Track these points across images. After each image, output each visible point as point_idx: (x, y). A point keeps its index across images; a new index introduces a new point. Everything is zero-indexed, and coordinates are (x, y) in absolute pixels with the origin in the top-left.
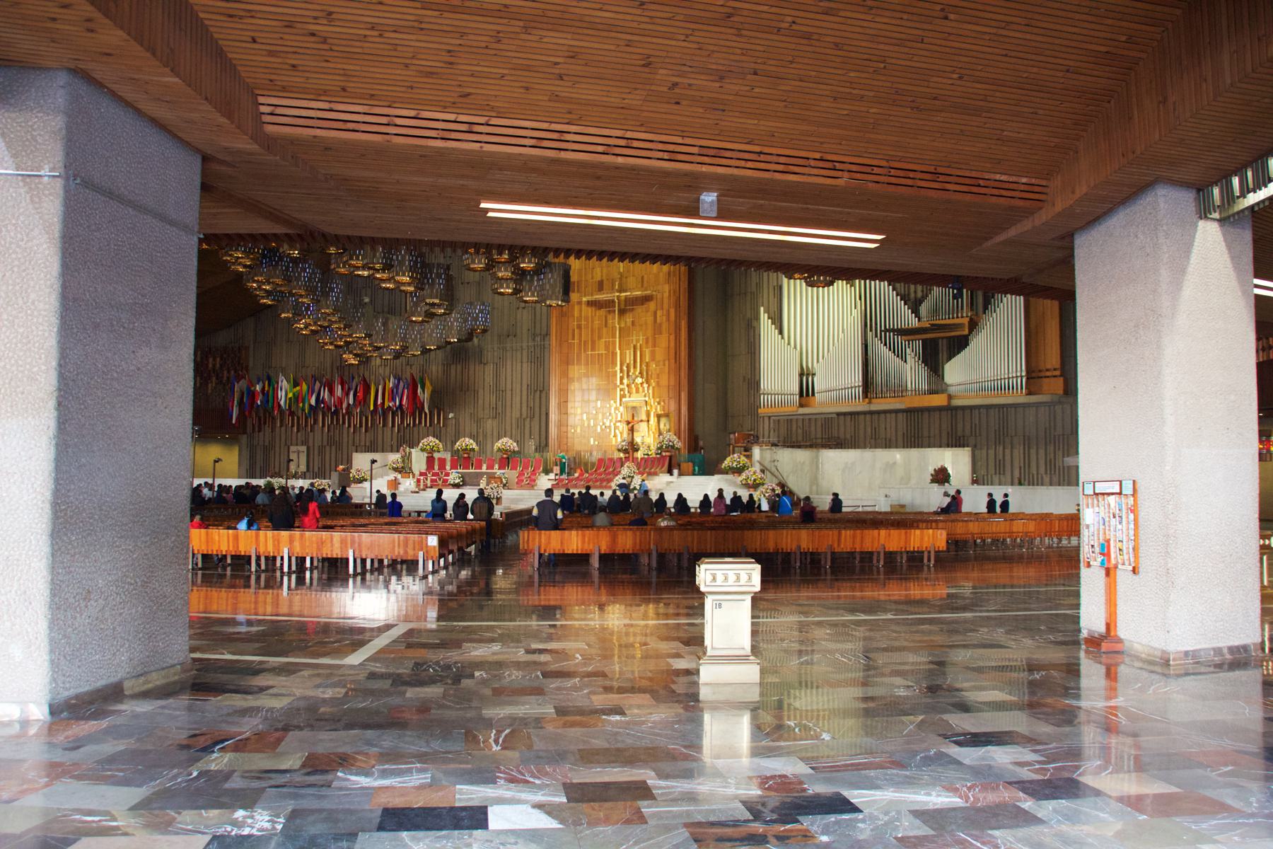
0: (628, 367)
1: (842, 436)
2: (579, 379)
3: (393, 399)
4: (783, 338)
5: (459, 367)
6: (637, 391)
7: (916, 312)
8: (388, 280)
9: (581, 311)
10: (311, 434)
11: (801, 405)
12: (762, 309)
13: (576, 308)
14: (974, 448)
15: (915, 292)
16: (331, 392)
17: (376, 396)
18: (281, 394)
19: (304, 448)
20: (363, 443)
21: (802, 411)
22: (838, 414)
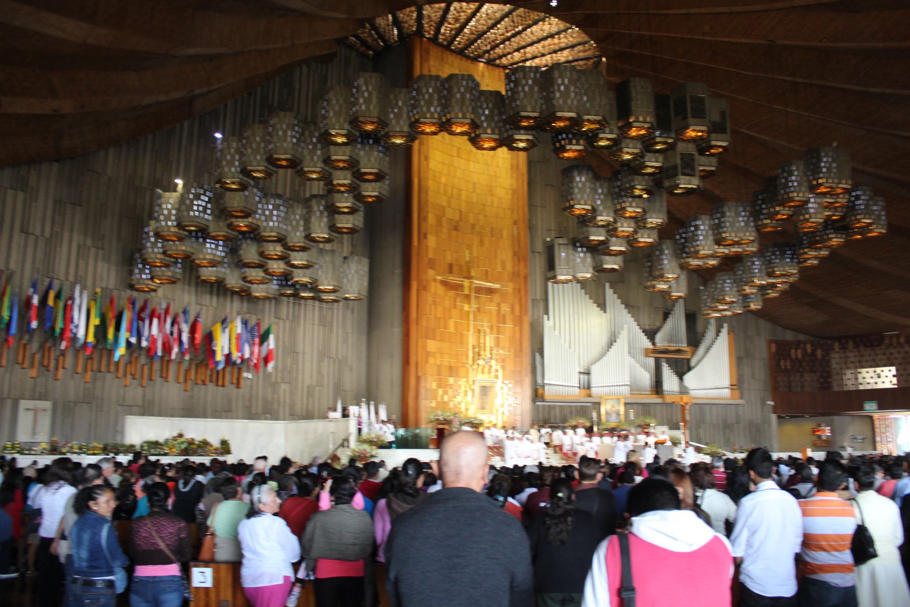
13: (433, 284)
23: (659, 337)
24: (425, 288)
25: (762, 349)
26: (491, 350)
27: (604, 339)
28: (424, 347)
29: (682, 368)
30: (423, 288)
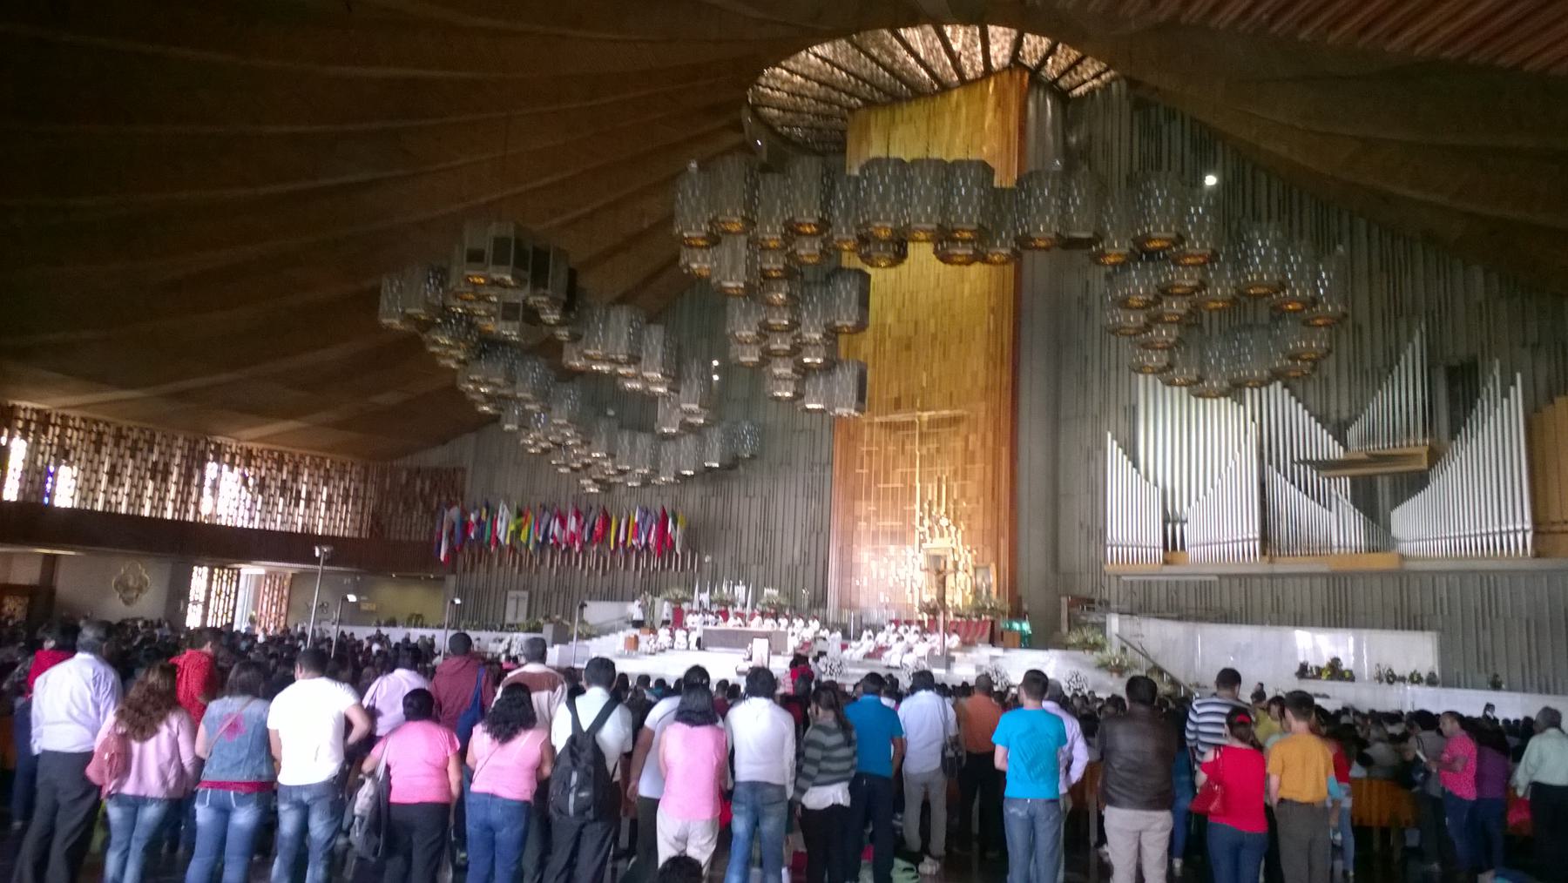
0: (930, 504)
1: (1226, 606)
2: (867, 519)
3: (637, 535)
4: (1138, 472)
5: (720, 501)
6: (942, 535)
7: (1340, 436)
8: (635, 378)
9: (872, 435)
10: (536, 578)
11: (1166, 562)
12: (1109, 435)
13: (867, 431)
14: (1441, 631)
15: (1338, 412)
16: (563, 524)
17: (618, 532)
18: (501, 526)
19: (525, 594)
20: (598, 589)
21: (1167, 569)
22: (1220, 576)
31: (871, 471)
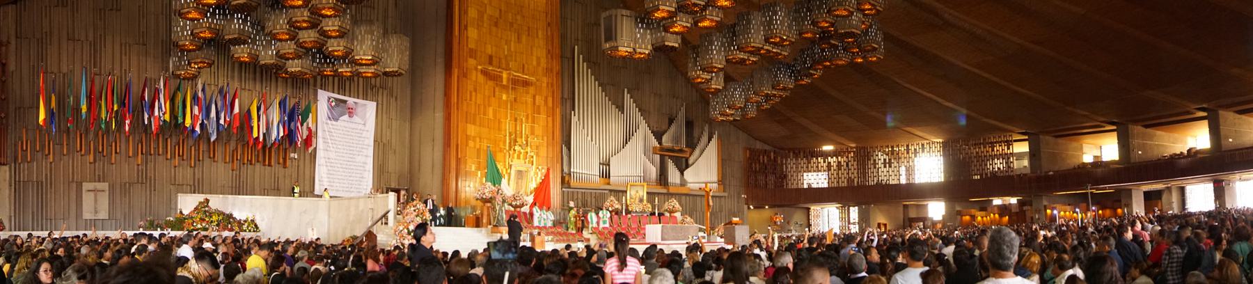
23: (665, 138)
24: (465, 75)
25: (739, 155)
26: (527, 137)
27: (621, 139)
28: (465, 131)
29: (683, 166)
30: (464, 75)
31: (476, 103)
